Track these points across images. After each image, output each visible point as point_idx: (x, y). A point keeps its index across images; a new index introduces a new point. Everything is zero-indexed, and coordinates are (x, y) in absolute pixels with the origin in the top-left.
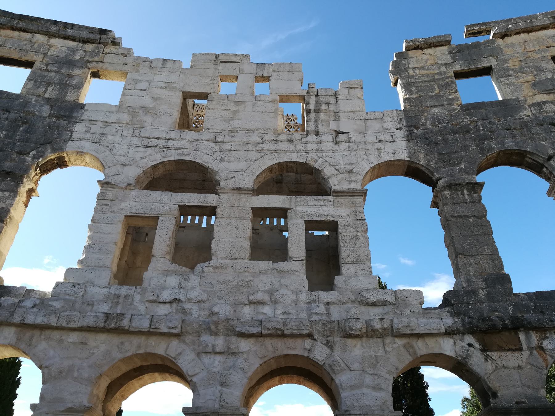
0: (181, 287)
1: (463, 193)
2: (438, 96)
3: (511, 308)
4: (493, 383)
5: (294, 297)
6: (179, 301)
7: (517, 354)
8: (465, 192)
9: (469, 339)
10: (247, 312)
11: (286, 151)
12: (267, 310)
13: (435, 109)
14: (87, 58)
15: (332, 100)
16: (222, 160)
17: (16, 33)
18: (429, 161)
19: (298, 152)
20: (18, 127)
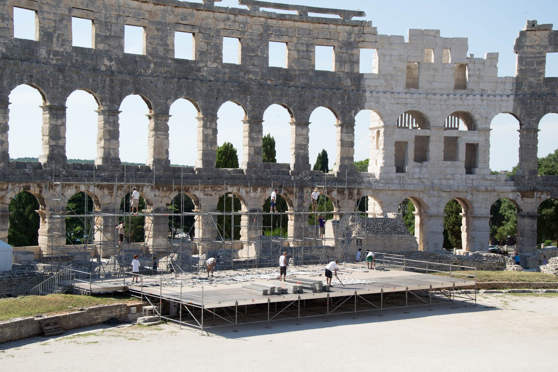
0: (420, 173)
1: (531, 133)
2: (535, 70)
3: (535, 184)
4: (522, 208)
5: (461, 177)
6: (421, 178)
7: (532, 199)
8: (532, 133)
9: (518, 193)
10: (444, 182)
11: (459, 105)
12: (451, 182)
13: (531, 78)
14: (357, 40)
15: (482, 67)
16: (430, 110)
17: (321, 25)
18: (521, 114)
19: (464, 105)
20: (344, 97)
